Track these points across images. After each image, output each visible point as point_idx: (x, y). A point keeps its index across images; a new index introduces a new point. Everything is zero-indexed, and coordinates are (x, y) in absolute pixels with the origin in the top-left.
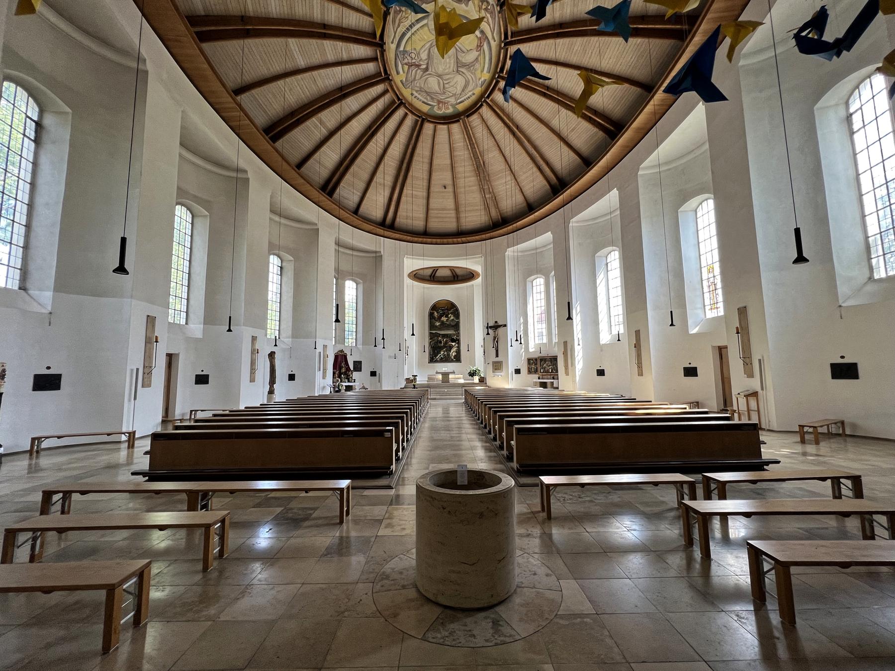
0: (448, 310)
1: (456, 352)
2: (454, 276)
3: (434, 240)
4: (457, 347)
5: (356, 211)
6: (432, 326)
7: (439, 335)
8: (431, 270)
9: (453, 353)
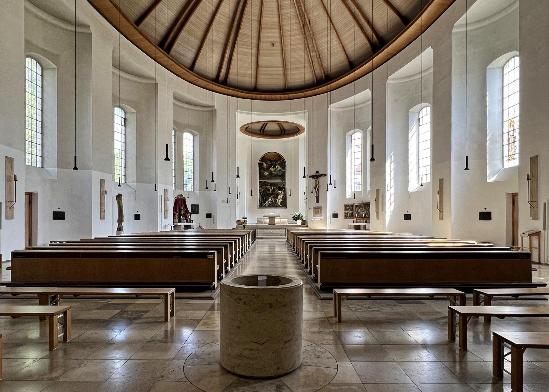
0: (276, 161)
1: (282, 199)
2: (282, 131)
3: (263, 96)
4: (283, 194)
5: (192, 68)
6: (261, 176)
7: (267, 184)
8: (261, 125)
9: (279, 200)
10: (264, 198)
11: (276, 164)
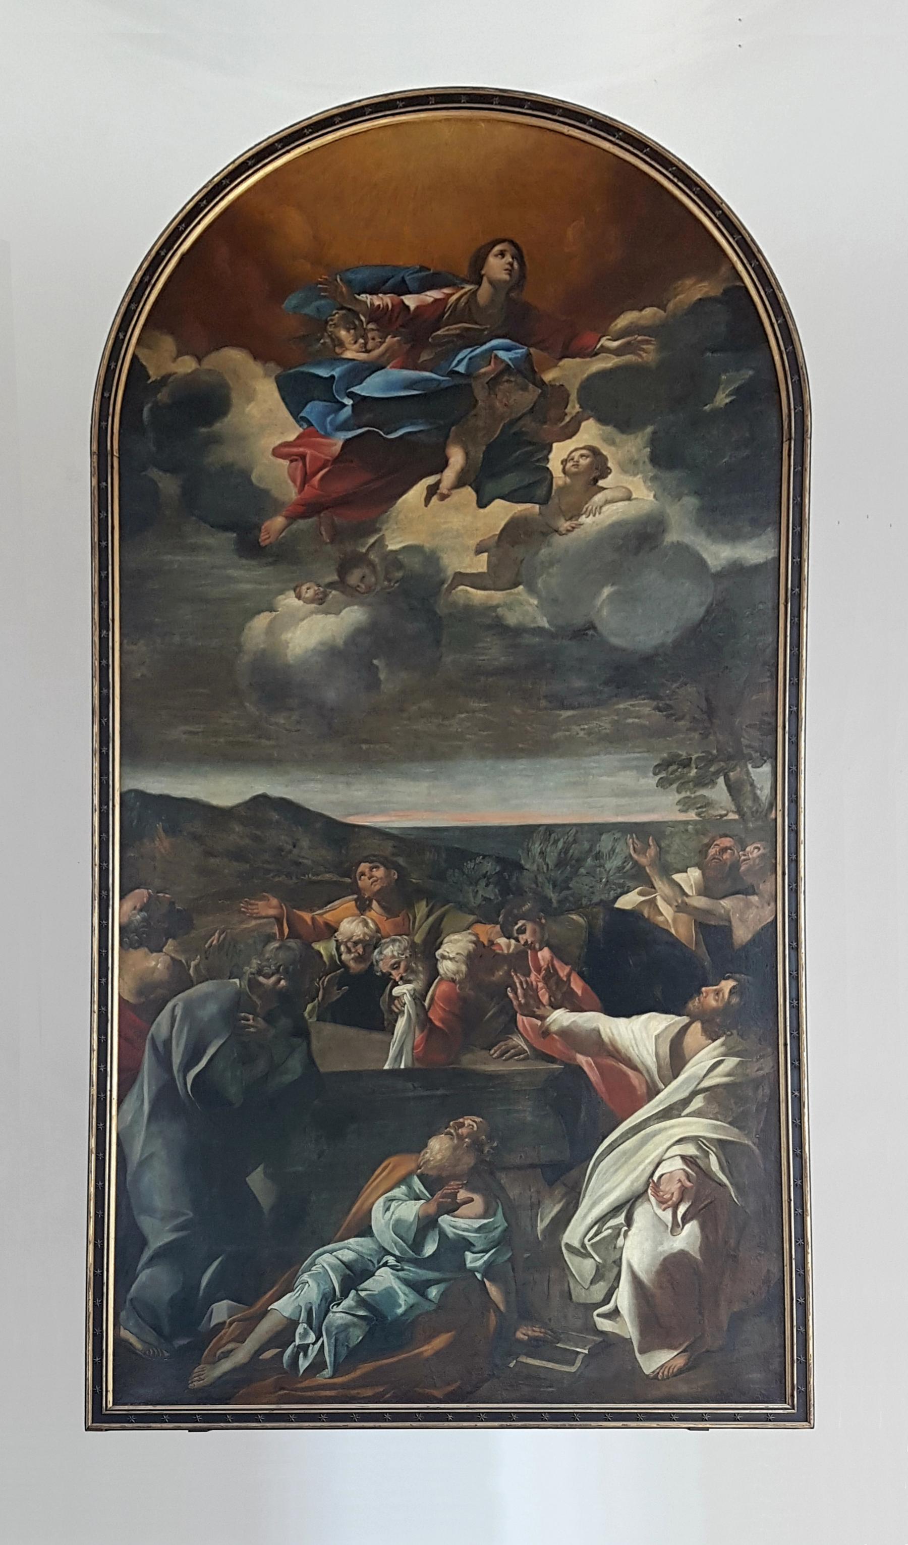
10: (257, 1180)
11: (558, 394)
